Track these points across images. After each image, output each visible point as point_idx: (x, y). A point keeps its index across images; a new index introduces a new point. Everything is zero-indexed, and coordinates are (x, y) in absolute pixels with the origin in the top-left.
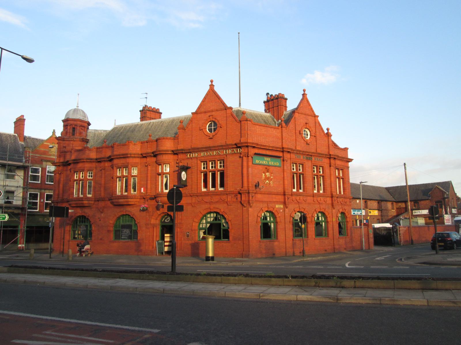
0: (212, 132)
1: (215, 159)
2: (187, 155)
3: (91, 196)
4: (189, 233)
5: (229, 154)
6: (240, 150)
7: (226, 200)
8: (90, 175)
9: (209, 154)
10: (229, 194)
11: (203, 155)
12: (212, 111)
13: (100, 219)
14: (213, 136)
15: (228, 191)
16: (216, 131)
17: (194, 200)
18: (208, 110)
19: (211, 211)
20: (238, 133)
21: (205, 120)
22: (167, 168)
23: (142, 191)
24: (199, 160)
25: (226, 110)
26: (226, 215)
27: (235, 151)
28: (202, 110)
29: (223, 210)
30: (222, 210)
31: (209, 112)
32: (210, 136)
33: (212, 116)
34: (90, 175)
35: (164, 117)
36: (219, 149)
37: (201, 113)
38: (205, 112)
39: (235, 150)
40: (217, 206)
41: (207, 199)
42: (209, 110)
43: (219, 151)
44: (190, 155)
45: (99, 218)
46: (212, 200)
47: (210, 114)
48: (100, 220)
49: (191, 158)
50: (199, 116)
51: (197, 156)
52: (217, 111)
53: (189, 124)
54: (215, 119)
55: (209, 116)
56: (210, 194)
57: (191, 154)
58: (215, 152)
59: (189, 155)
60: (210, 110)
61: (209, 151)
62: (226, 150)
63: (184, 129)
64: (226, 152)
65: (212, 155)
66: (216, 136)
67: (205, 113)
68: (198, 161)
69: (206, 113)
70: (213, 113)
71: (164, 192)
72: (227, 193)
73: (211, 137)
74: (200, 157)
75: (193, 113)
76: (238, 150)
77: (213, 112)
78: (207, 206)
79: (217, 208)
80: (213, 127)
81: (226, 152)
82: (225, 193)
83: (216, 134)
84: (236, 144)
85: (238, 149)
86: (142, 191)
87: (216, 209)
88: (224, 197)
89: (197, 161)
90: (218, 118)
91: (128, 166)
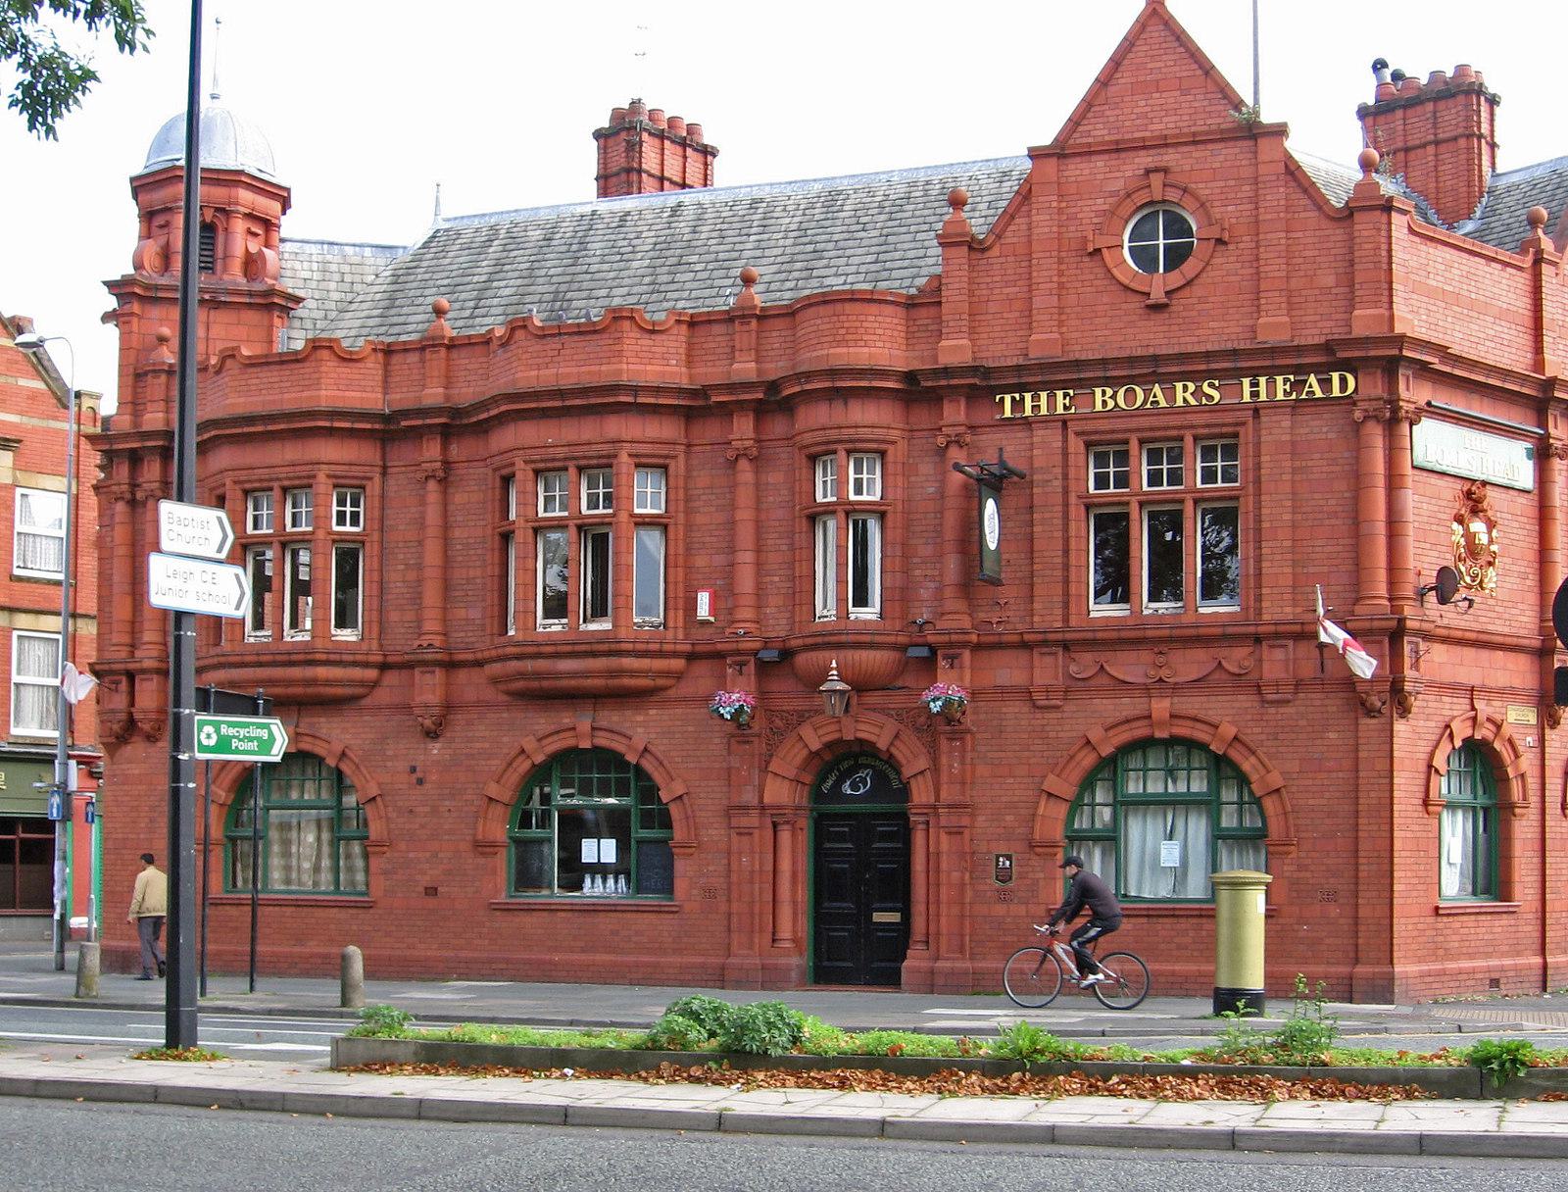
0: (1157, 270)
2: (1002, 400)
4: (1009, 858)
5: (1273, 405)
6: (1343, 381)
7: (1254, 676)
9: (1145, 402)
10: (1277, 635)
11: (1104, 403)
12: (1164, 143)
14: (1168, 293)
15: (1266, 617)
16: (1190, 267)
17: (1046, 670)
18: (1137, 135)
19: (1158, 734)
20: (1329, 280)
21: (1112, 194)
22: (865, 476)
24: (1077, 434)
25: (1251, 143)
26: (1253, 759)
28: (1098, 132)
29: (1231, 731)
30: (1228, 730)
31: (1144, 148)
32: (1148, 294)
33: (1165, 171)
34: (348, 509)
35: (723, 172)
36: (1209, 374)
37: (1088, 153)
38: (1118, 149)
39: (1312, 379)
40: (1191, 704)
41: (1131, 667)
42: (1143, 139)
43: (1211, 385)
44: (1023, 399)
46: (1164, 673)
47: (1150, 159)
49: (1027, 423)
50: (1076, 169)
51: (1066, 408)
52: (1195, 143)
53: (1009, 216)
54: (1185, 190)
55: (1148, 172)
56: (1150, 633)
57: (1028, 396)
58: (1185, 389)
59: (1013, 399)
60: (1148, 134)
61: (1145, 383)
62: (1255, 376)
63: (975, 247)
64: (1255, 394)
65: (1163, 403)
66: (1186, 292)
67: (1117, 150)
68: (1071, 437)
69: (1123, 155)
70: (1169, 158)
71: (852, 617)
72: (1261, 629)
73: (1157, 295)
74: (1085, 418)
75: (1035, 154)
77: (1170, 150)
78: (1128, 706)
79: (1195, 719)
80: (1161, 242)
81: (1255, 394)
82: (1252, 629)
83: (1189, 283)
84: (1328, 347)
85: (1335, 376)
87: (1190, 723)
88: (1236, 658)
89: (1065, 440)
90: (1200, 185)
91: (615, 462)
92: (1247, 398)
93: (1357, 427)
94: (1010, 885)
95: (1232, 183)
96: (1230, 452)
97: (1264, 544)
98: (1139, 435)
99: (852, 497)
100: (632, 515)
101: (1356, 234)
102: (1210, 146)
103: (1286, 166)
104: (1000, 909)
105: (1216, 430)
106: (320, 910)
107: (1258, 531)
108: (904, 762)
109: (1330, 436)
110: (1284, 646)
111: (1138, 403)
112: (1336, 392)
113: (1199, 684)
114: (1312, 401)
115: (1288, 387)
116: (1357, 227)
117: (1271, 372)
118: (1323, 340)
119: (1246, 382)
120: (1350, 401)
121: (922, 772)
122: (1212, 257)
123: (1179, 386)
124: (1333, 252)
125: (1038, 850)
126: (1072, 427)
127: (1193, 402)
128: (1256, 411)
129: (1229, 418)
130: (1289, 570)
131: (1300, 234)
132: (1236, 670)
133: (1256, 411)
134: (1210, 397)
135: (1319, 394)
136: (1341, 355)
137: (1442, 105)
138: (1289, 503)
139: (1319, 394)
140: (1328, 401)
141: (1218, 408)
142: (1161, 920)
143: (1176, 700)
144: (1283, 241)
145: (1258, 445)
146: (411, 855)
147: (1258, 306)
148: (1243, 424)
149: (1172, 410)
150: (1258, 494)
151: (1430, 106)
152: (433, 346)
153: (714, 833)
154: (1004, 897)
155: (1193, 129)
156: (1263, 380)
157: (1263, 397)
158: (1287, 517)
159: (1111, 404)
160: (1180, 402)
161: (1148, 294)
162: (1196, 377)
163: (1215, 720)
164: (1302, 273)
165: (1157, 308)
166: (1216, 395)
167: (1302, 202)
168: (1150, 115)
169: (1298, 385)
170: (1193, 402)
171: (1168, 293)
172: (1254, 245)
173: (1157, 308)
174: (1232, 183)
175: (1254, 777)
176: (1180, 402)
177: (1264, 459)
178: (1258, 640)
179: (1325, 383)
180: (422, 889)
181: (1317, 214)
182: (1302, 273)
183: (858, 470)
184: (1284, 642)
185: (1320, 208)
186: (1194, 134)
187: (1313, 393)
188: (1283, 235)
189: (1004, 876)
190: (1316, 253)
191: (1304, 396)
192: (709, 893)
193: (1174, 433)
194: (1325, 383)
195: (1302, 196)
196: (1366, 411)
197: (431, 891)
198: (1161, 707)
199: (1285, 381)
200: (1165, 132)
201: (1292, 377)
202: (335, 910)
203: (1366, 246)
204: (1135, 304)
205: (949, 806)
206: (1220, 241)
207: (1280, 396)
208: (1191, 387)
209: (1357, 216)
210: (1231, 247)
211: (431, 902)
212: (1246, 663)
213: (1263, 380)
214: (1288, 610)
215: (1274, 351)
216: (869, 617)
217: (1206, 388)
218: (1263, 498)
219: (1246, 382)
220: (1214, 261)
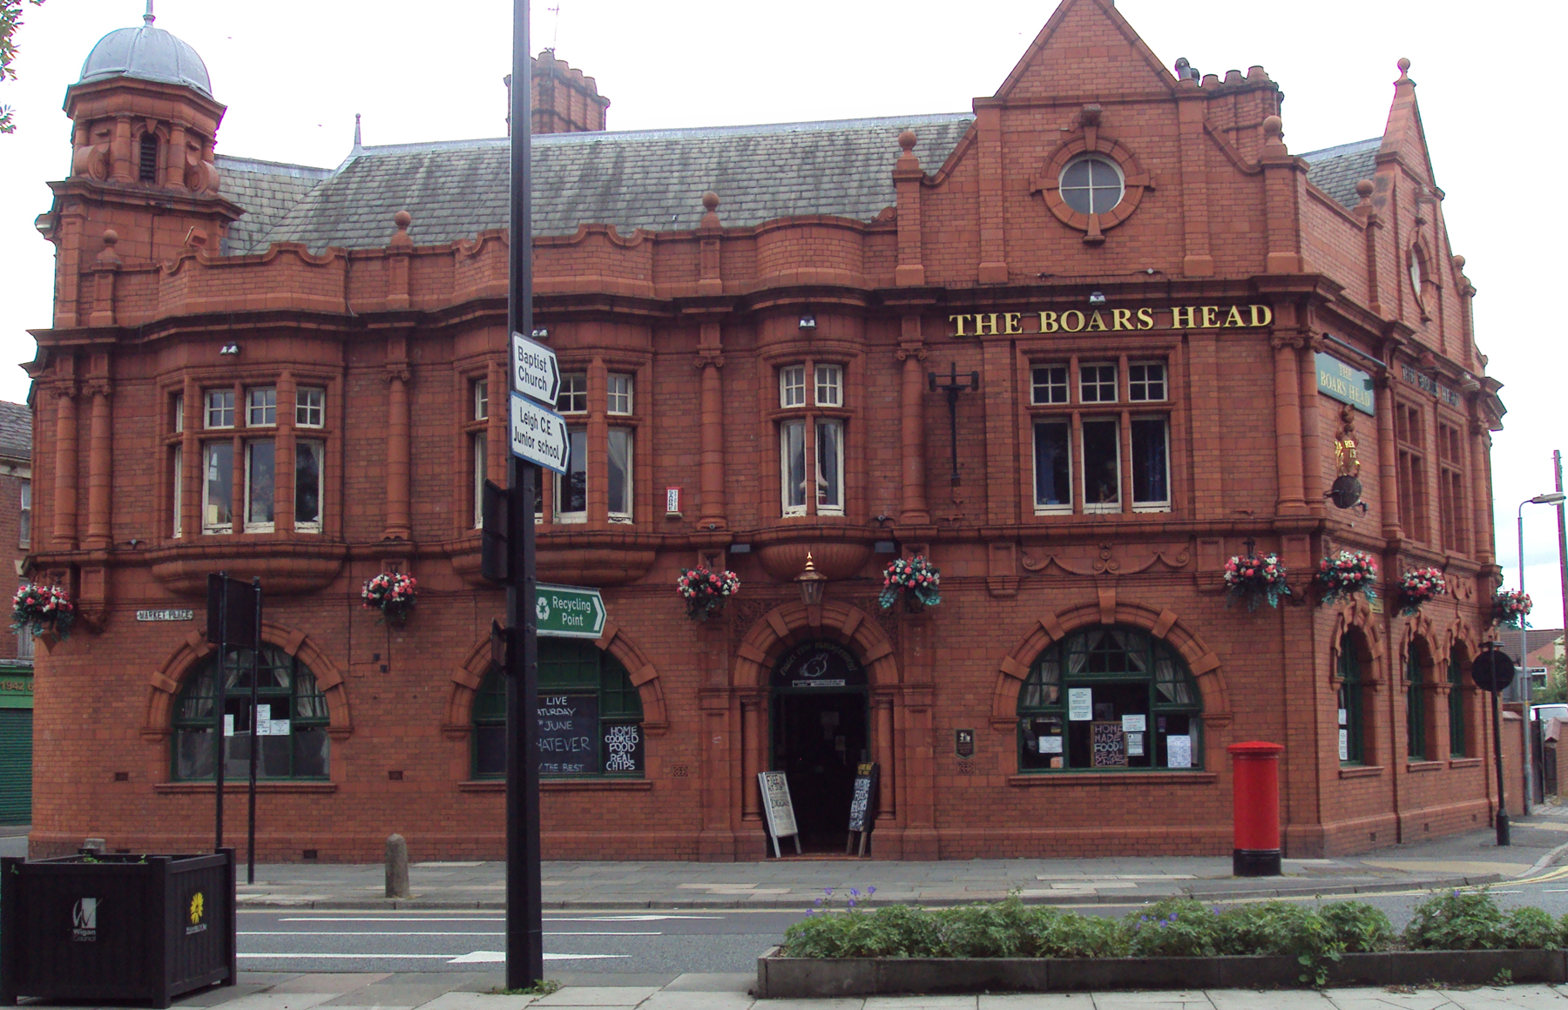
1: (1118, 349)
2: (955, 320)
3: (315, 531)
4: (969, 733)
5: (1200, 332)
7: (1190, 569)
8: (309, 407)
9: (1086, 326)
11: (1049, 326)
13: (383, 662)
14: (1104, 231)
15: (1199, 517)
17: (1004, 564)
21: (1050, 143)
23: (673, 506)
24: (1024, 352)
25: (1173, 106)
26: (1191, 643)
27: (1238, 318)
28: (1035, 88)
30: (1170, 617)
35: (618, 121)
37: (1028, 106)
38: (1054, 104)
39: (1234, 310)
40: (1134, 594)
41: (1078, 561)
43: (1145, 313)
44: (974, 320)
48: (385, 669)
49: (979, 342)
50: (1019, 121)
51: (1014, 328)
52: (1123, 103)
53: (956, 159)
54: (1116, 143)
57: (979, 318)
58: (1122, 315)
59: (965, 320)
60: (1081, 93)
63: (927, 184)
64: (1184, 322)
66: (1118, 232)
67: (1054, 106)
69: (1058, 110)
71: (820, 513)
74: (1032, 338)
75: (979, 105)
76: (1249, 313)
78: (1075, 595)
79: (1138, 607)
80: (1091, 187)
81: (1184, 322)
84: (1252, 283)
86: (673, 506)
87: (1133, 611)
88: (1174, 554)
89: (1013, 357)
90: (1129, 140)
92: (1177, 325)
93: (1274, 351)
94: (971, 758)
95: (1157, 139)
96: (1156, 373)
97: (1195, 453)
98: (1079, 355)
99: (818, 404)
100: (607, 417)
101: (1268, 188)
102: (1136, 107)
103: (1205, 128)
104: (962, 781)
105: (1149, 352)
106: (279, 796)
107: (1190, 441)
108: (867, 646)
109: (1249, 360)
110: (1217, 543)
111: (1081, 326)
112: (1255, 322)
113: (1143, 576)
114: (1234, 329)
115: (1212, 316)
116: (1268, 182)
117: (1198, 304)
118: (1246, 277)
119: (1176, 311)
120: (1268, 331)
121: (886, 656)
122: (1140, 202)
123: (1116, 312)
124: (1247, 202)
125: (997, 726)
126: (1020, 346)
127: (1129, 327)
129: (1159, 342)
130: (1217, 476)
131: (1218, 186)
132: (1172, 563)
134: (1145, 324)
135: (1240, 323)
136: (1262, 290)
137: (1241, 98)
138: (1216, 418)
140: (1249, 330)
141: (1152, 333)
142: (1112, 788)
143: (1120, 589)
144: (1204, 191)
145: (1187, 365)
146: (376, 740)
147: (1184, 246)
148: (1173, 348)
149: (1111, 333)
150: (1189, 409)
151: (1231, 99)
153: (686, 714)
154: (964, 770)
155: (1121, 91)
156: (1191, 310)
157: (1191, 324)
158: (1215, 429)
159: (1055, 327)
160: (1117, 327)
161: (1086, 232)
162: (1134, 306)
163: (1157, 607)
164: (1220, 219)
165: (1094, 244)
166: (1150, 321)
167: (1218, 159)
168: (1082, 77)
169: (1222, 315)
170: (1129, 327)
171: (1104, 231)
172: (1177, 193)
173: (1094, 244)
174: (1157, 139)
175: (1192, 659)
176: (1117, 327)
177: (1194, 378)
178: (1192, 537)
179: (1246, 315)
180: (385, 774)
181: (1231, 169)
182: (1220, 219)
184: (1215, 539)
185: (1235, 165)
186: (1123, 95)
187: (1235, 322)
188: (1203, 185)
189: (965, 750)
190: (1232, 202)
191: (1227, 325)
192: (681, 771)
193: (1110, 353)
194: (1246, 315)
195: (1218, 153)
196: (1283, 339)
197: (396, 775)
198: (1107, 596)
199: (1211, 311)
200: (1096, 92)
201: (1216, 308)
202: (296, 796)
203: (1277, 199)
204: (1074, 241)
205: (913, 687)
206: (1148, 189)
207: (1206, 324)
208: (1128, 313)
209: (1268, 173)
210: (1156, 193)
211: (395, 786)
212: (1183, 558)
213: (1191, 310)
214: (1219, 511)
216: (835, 513)
217: (1141, 315)
218: (1194, 412)
219: (1176, 311)
220: (1142, 205)
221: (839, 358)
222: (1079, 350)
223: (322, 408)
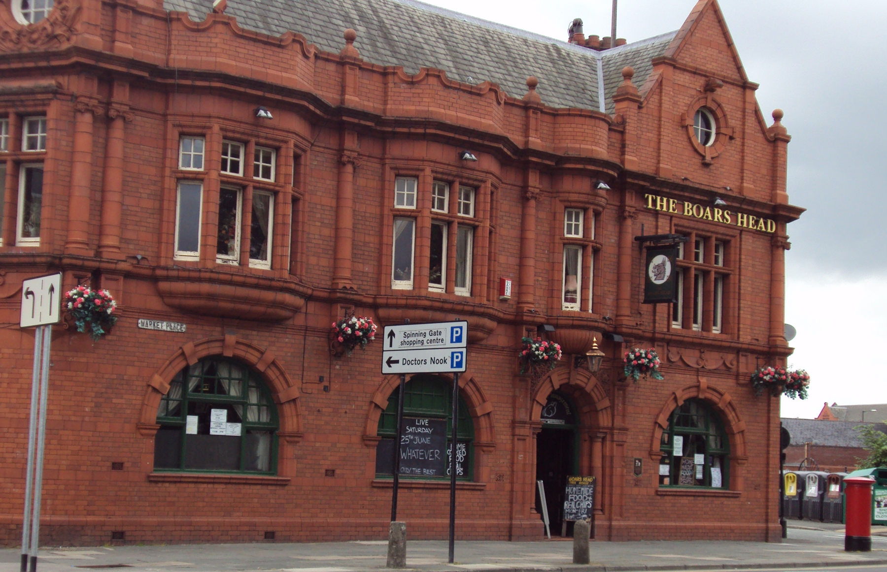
1: (712, 232)
2: (648, 197)
4: (640, 460)
13: (326, 383)
22: (573, 223)
34: (229, 158)
44: (656, 198)
45: (321, 379)
48: (326, 389)
59: (652, 198)
94: (640, 476)
106: (247, 487)
119: (740, 215)
126: (675, 221)
127: (721, 221)
128: (741, 231)
129: (730, 232)
133: (741, 231)
139: (764, 229)
140: (766, 233)
141: (729, 227)
146: (318, 444)
152: (353, 64)
153: (503, 437)
159: (690, 214)
160: (716, 220)
177: (743, 257)
180: (324, 471)
183: (570, 219)
189: (637, 471)
197: (330, 473)
199: (753, 219)
202: (259, 487)
205: (620, 429)
208: (721, 213)
211: (331, 481)
215: (751, 203)
221: (581, 205)
222: (697, 229)
223: (273, 166)
